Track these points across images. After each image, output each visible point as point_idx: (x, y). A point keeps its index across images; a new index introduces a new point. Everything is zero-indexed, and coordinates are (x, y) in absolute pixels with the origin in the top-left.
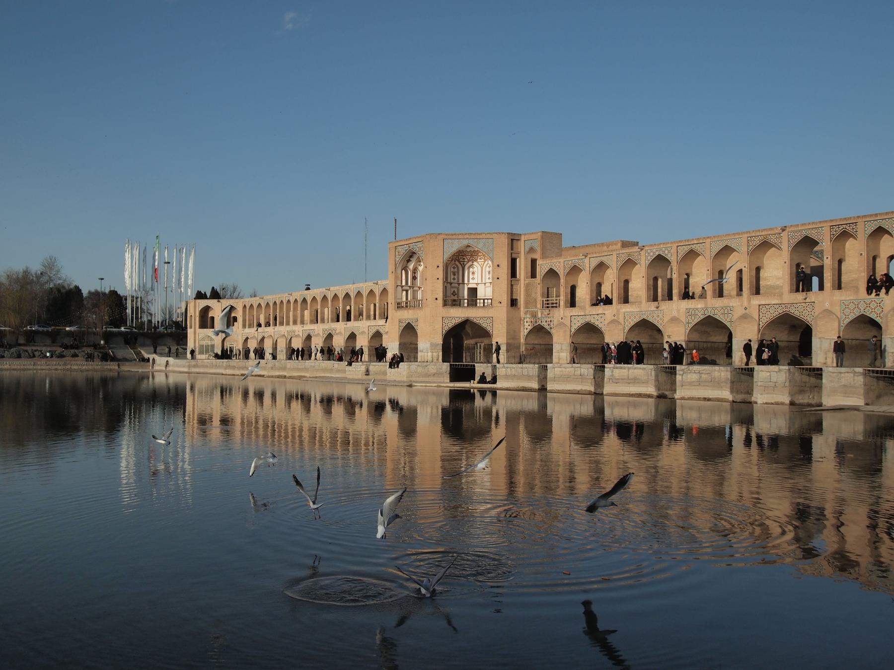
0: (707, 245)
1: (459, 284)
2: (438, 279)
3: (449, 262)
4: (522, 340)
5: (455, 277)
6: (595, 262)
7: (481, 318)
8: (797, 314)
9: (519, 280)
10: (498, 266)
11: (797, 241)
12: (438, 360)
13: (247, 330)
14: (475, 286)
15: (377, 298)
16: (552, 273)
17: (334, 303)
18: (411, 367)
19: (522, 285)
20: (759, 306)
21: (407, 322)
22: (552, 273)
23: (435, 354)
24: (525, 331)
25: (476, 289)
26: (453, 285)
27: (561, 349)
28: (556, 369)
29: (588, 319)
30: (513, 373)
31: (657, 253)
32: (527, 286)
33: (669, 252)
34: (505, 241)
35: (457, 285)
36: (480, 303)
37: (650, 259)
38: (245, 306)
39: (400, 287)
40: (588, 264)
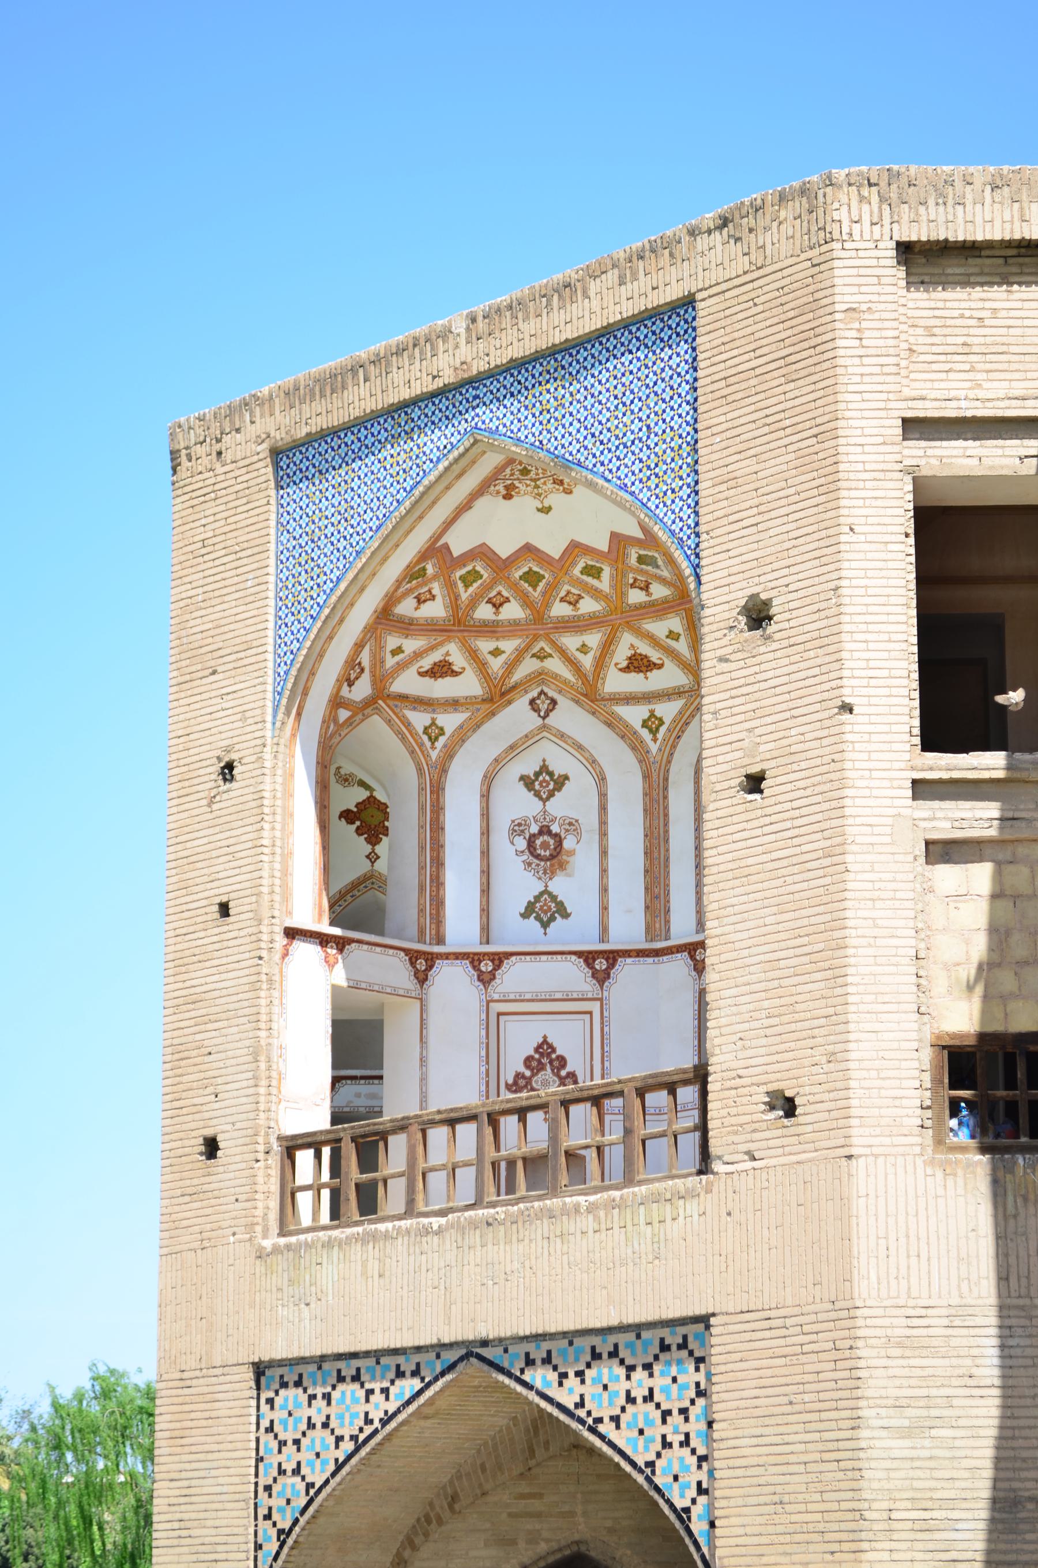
2: (224, 910)
3: (450, 721)
5: (559, 885)
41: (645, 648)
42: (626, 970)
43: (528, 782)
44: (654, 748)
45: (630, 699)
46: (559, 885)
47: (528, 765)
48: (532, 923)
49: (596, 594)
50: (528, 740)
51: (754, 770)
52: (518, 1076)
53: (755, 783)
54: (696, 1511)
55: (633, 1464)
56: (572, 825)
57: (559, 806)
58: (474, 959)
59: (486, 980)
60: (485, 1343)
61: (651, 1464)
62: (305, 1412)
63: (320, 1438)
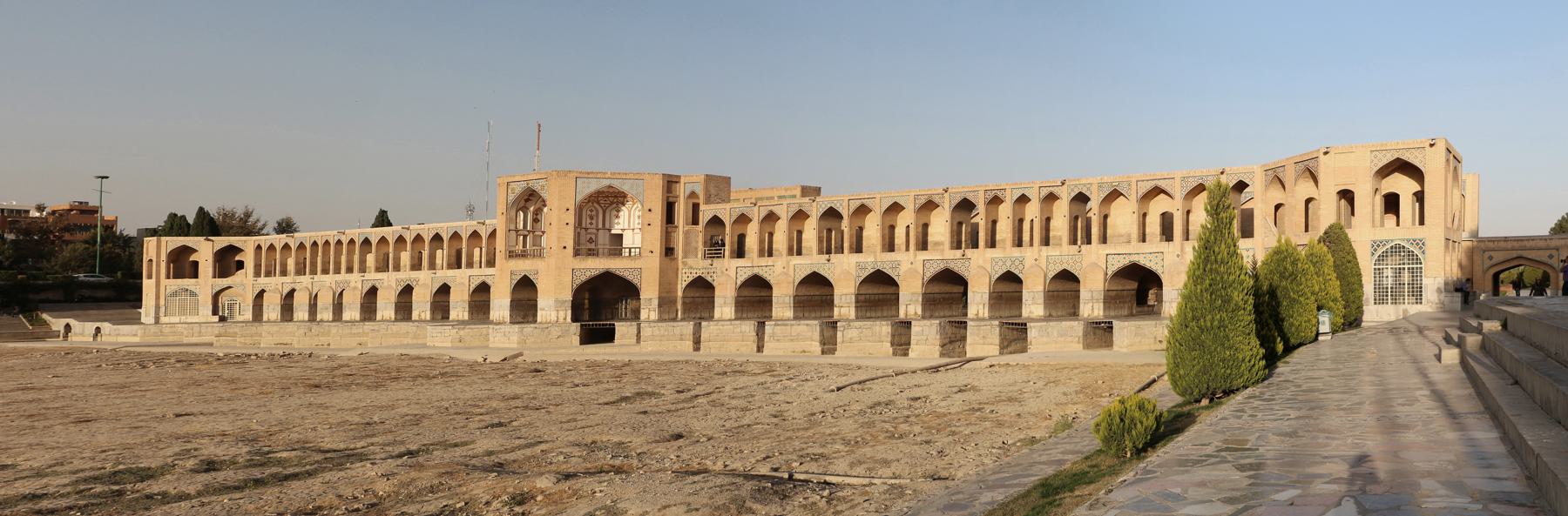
0: (877, 201)
4: (680, 293)
6: (764, 213)
8: (956, 269)
9: (676, 227)
11: (957, 202)
13: (263, 281)
14: (620, 232)
15: (484, 242)
16: (716, 222)
17: (415, 245)
19: (681, 233)
20: (924, 261)
22: (716, 222)
24: (684, 282)
25: (621, 235)
27: (725, 303)
29: (756, 271)
31: (829, 206)
32: (686, 234)
33: (841, 205)
34: (659, 183)
36: (626, 253)
37: (822, 211)
38: (259, 247)
40: (757, 215)
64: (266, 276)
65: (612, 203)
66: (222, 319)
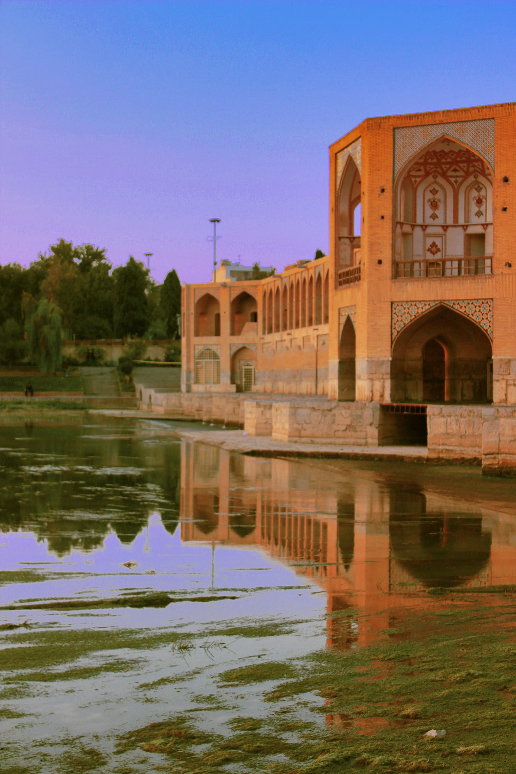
1: (445, 228)
2: (383, 217)
3: (418, 180)
5: (437, 212)
7: (470, 301)
10: (506, 180)
12: (382, 396)
14: (479, 230)
18: (300, 411)
21: (347, 314)
23: (378, 385)
26: (429, 230)
28: (502, 421)
30: (463, 429)
35: (440, 230)
39: (347, 241)
41: (457, 168)
42: (450, 229)
43: (431, 191)
44: (456, 186)
45: (452, 177)
46: (437, 212)
47: (431, 188)
48: (432, 219)
49: (451, 158)
50: (432, 183)
51: (505, 207)
52: (429, 248)
53: (505, 209)
54: (489, 330)
55: (476, 322)
56: (439, 200)
57: (437, 196)
58: (422, 226)
59: (424, 230)
60: (445, 300)
61: (480, 322)
62: (403, 311)
63: (406, 315)
64: (283, 331)
65: (467, 174)
66: (239, 390)
